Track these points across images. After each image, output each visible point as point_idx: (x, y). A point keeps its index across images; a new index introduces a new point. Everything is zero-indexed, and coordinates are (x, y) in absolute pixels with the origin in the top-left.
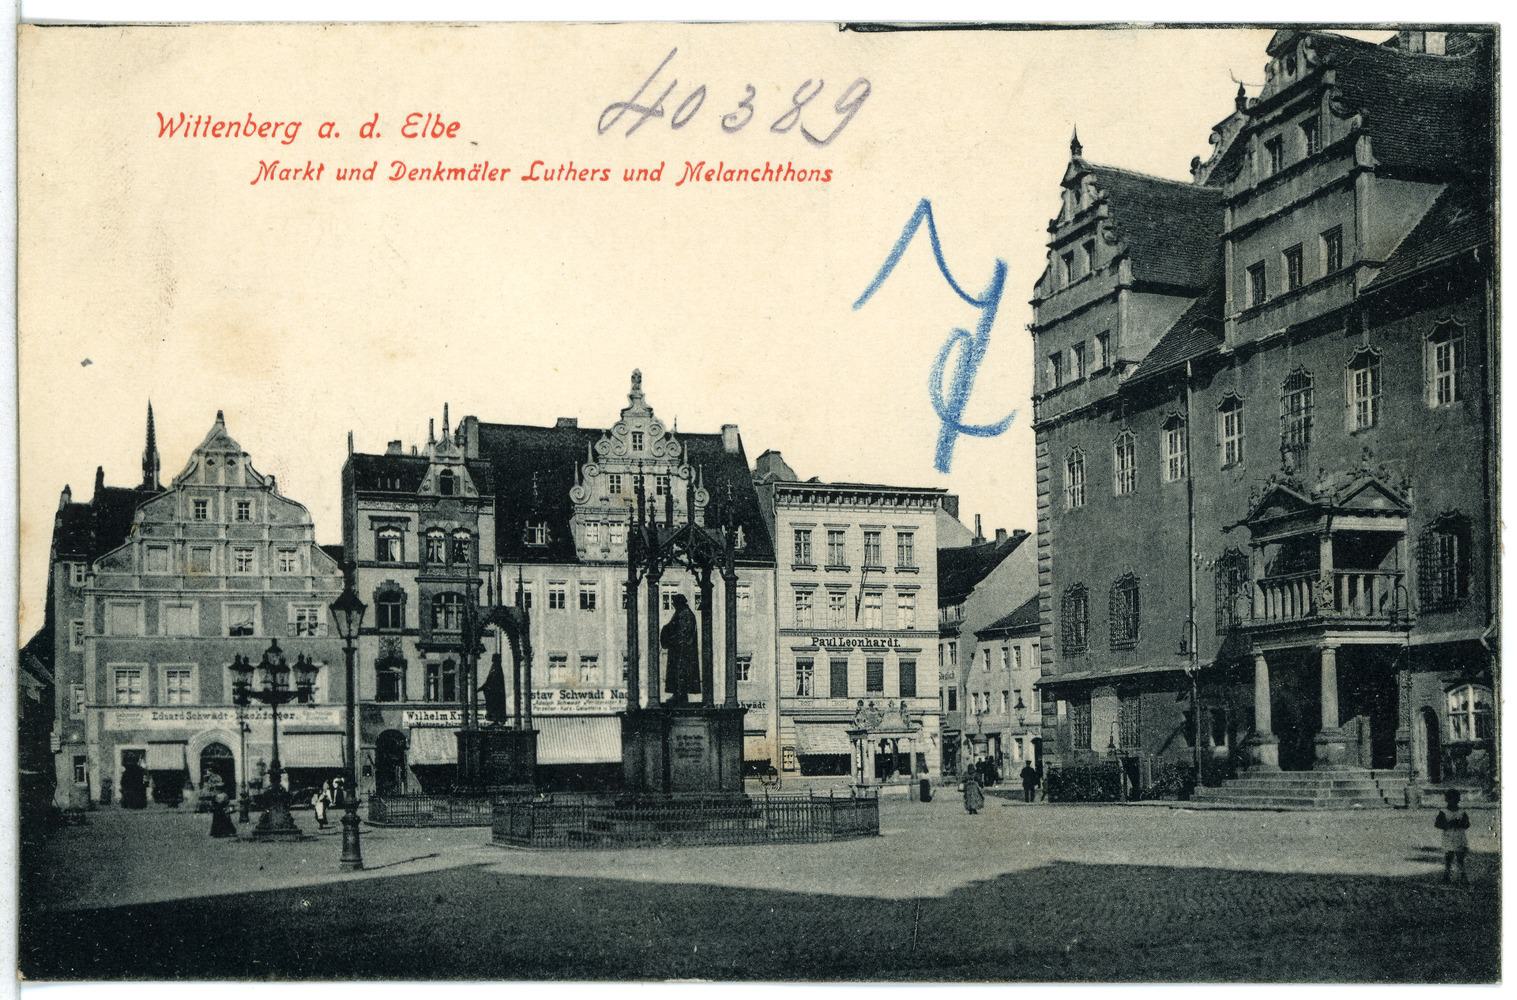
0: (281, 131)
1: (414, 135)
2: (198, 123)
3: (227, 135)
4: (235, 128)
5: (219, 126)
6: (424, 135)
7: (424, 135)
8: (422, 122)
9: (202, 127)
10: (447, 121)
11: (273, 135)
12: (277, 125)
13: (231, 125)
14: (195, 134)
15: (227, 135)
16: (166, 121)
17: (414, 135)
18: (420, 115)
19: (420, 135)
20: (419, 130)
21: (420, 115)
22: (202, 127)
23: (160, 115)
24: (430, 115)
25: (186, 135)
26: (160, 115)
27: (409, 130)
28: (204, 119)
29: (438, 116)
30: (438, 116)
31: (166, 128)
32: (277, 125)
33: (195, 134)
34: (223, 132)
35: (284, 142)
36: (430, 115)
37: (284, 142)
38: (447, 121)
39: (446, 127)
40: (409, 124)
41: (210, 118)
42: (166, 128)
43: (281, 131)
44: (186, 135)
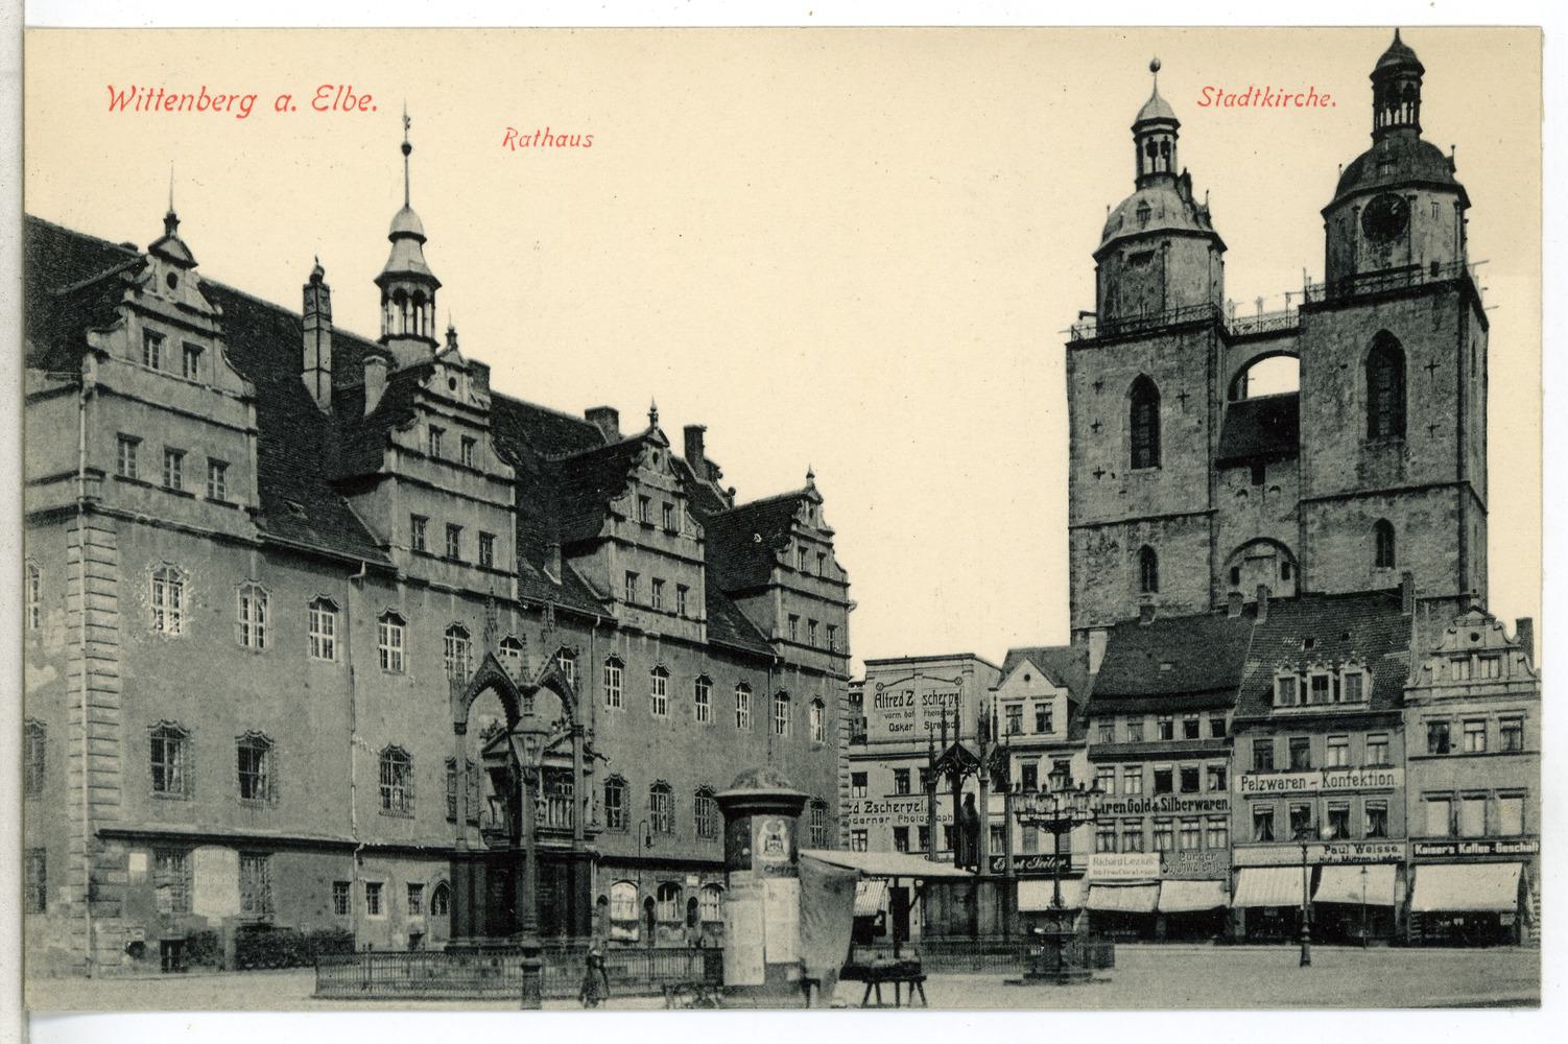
0: (236, 104)
1: (326, 108)
2: (150, 96)
3: (180, 108)
6: (335, 108)
7: (335, 108)
8: (334, 94)
9: (154, 100)
10: (358, 93)
11: (228, 109)
12: (232, 98)
14: (147, 108)
15: (180, 108)
16: (117, 94)
17: (326, 108)
18: (332, 88)
20: (329, 102)
21: (332, 88)
22: (154, 100)
23: (110, 88)
24: (341, 88)
25: (137, 109)
26: (110, 88)
27: (320, 103)
28: (157, 92)
29: (350, 88)
30: (350, 88)
31: (118, 101)
32: (232, 98)
33: (147, 108)
34: (175, 106)
35: (238, 116)
36: (341, 88)
37: (238, 116)
38: (358, 93)
40: (320, 96)
42: (118, 101)
43: (236, 104)
44: (137, 109)
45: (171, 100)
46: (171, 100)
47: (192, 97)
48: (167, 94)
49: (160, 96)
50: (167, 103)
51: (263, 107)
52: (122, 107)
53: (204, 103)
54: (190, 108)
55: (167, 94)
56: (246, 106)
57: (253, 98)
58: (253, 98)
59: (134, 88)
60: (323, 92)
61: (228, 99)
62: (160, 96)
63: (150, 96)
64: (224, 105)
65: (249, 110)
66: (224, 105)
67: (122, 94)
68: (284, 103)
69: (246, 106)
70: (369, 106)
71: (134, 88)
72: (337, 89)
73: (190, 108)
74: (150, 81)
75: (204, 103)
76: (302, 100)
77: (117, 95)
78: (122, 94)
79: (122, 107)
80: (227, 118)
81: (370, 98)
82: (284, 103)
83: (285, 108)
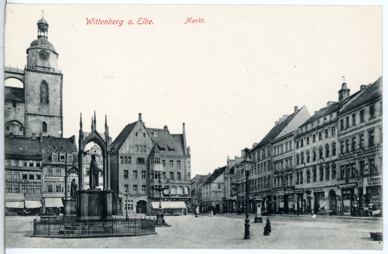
0: (118, 22)
1: (141, 24)
2: (97, 21)
3: (104, 24)
4: (106, 22)
5: (102, 22)
6: (143, 24)
7: (143, 24)
9: (98, 22)
10: (149, 20)
11: (116, 24)
12: (117, 21)
13: (105, 21)
14: (96, 24)
15: (104, 24)
16: (89, 21)
17: (141, 24)
18: (142, 19)
19: (142, 23)
20: (142, 22)
21: (142, 19)
23: (87, 19)
24: (144, 18)
25: (94, 24)
26: (87, 19)
27: (139, 22)
28: (99, 20)
29: (147, 19)
30: (147, 19)
31: (89, 22)
32: (117, 21)
33: (96, 24)
35: (119, 26)
36: (144, 18)
37: (119, 26)
38: (149, 20)
39: (149, 22)
41: (100, 19)
42: (89, 22)
43: (118, 22)
44: (94, 24)
45: (114, 21)
46: (102, 22)
47: (108, 21)
48: (101, 20)
49: (99, 21)
50: (101, 23)
51: (125, 24)
52: (90, 23)
53: (110, 22)
54: (107, 24)
55: (101, 20)
56: (121, 23)
57: (123, 21)
58: (123, 21)
59: (93, 19)
60: (140, 20)
61: (116, 21)
62: (99, 21)
63: (97, 21)
64: (115, 23)
65: (121, 24)
66: (115, 23)
67: (90, 20)
68: (130, 22)
69: (121, 23)
70: (151, 23)
71: (93, 19)
72: (143, 19)
73: (107, 24)
74: (96, 17)
75: (147, 22)
76: (135, 22)
77: (89, 21)
78: (90, 20)
79: (90, 23)
80: (116, 26)
81: (152, 21)
82: (130, 22)
83: (131, 24)
